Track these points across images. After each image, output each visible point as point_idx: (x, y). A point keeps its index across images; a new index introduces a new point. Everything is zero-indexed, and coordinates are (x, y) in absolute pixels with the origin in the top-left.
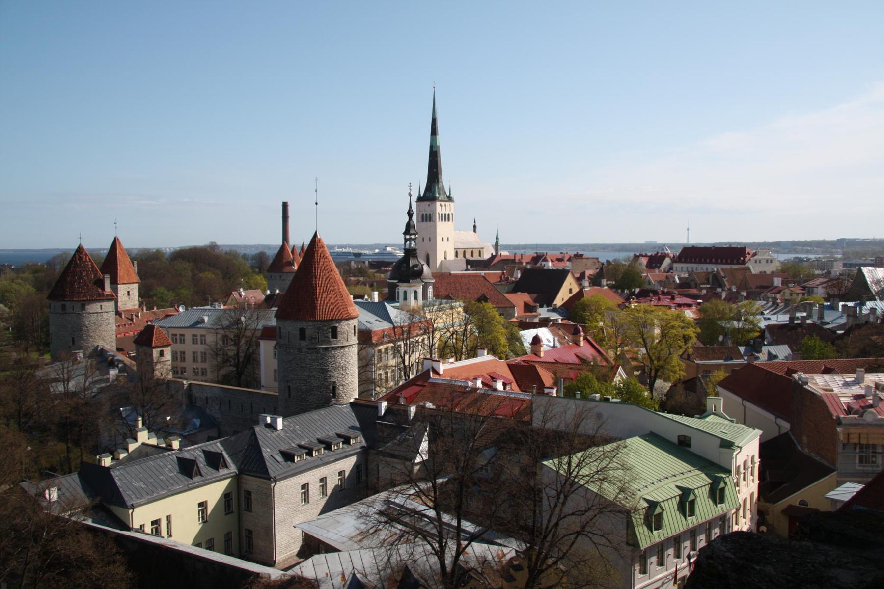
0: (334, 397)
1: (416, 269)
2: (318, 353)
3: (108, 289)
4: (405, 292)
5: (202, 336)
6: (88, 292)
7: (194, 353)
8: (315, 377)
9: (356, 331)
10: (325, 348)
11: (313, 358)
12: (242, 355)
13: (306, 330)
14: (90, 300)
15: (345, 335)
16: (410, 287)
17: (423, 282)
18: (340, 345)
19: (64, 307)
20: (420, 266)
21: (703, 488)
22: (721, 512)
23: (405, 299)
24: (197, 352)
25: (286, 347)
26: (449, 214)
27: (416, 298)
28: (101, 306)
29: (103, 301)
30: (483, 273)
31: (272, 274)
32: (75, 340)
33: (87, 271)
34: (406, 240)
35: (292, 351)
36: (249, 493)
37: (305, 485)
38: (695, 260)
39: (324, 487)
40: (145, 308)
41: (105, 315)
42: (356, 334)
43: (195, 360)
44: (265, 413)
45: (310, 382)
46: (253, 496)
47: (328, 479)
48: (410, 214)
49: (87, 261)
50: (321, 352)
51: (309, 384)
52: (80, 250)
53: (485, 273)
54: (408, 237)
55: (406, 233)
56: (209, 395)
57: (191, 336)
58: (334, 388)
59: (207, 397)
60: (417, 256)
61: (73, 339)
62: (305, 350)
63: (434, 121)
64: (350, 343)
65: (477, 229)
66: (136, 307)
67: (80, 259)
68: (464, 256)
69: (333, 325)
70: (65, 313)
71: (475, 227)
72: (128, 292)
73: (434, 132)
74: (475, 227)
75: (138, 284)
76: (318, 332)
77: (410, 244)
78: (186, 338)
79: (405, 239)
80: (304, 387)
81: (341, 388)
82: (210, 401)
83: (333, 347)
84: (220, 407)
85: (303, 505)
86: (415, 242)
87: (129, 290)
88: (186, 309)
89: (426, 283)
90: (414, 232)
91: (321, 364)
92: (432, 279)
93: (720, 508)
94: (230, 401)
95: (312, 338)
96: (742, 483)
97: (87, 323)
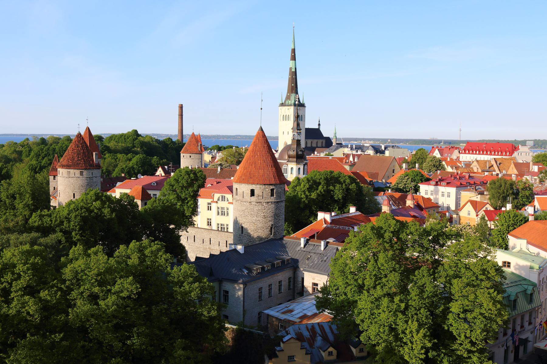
0: (271, 234)
5: (154, 195)
6: (84, 164)
8: (260, 221)
11: (260, 208)
21: (521, 293)
22: (531, 308)
27: (299, 173)
30: (330, 157)
31: (184, 154)
35: (245, 203)
36: (227, 292)
37: (260, 288)
38: (483, 152)
39: (270, 290)
41: (94, 179)
46: (230, 294)
47: (272, 285)
50: (264, 205)
52: (79, 135)
53: (333, 158)
61: (74, 194)
63: (294, 51)
64: (282, 200)
65: (321, 126)
68: (311, 145)
69: (271, 188)
71: (319, 125)
73: (294, 58)
74: (319, 125)
80: (253, 227)
83: (272, 202)
85: (259, 301)
89: (306, 163)
93: (530, 306)
94: (194, 236)
96: (541, 292)
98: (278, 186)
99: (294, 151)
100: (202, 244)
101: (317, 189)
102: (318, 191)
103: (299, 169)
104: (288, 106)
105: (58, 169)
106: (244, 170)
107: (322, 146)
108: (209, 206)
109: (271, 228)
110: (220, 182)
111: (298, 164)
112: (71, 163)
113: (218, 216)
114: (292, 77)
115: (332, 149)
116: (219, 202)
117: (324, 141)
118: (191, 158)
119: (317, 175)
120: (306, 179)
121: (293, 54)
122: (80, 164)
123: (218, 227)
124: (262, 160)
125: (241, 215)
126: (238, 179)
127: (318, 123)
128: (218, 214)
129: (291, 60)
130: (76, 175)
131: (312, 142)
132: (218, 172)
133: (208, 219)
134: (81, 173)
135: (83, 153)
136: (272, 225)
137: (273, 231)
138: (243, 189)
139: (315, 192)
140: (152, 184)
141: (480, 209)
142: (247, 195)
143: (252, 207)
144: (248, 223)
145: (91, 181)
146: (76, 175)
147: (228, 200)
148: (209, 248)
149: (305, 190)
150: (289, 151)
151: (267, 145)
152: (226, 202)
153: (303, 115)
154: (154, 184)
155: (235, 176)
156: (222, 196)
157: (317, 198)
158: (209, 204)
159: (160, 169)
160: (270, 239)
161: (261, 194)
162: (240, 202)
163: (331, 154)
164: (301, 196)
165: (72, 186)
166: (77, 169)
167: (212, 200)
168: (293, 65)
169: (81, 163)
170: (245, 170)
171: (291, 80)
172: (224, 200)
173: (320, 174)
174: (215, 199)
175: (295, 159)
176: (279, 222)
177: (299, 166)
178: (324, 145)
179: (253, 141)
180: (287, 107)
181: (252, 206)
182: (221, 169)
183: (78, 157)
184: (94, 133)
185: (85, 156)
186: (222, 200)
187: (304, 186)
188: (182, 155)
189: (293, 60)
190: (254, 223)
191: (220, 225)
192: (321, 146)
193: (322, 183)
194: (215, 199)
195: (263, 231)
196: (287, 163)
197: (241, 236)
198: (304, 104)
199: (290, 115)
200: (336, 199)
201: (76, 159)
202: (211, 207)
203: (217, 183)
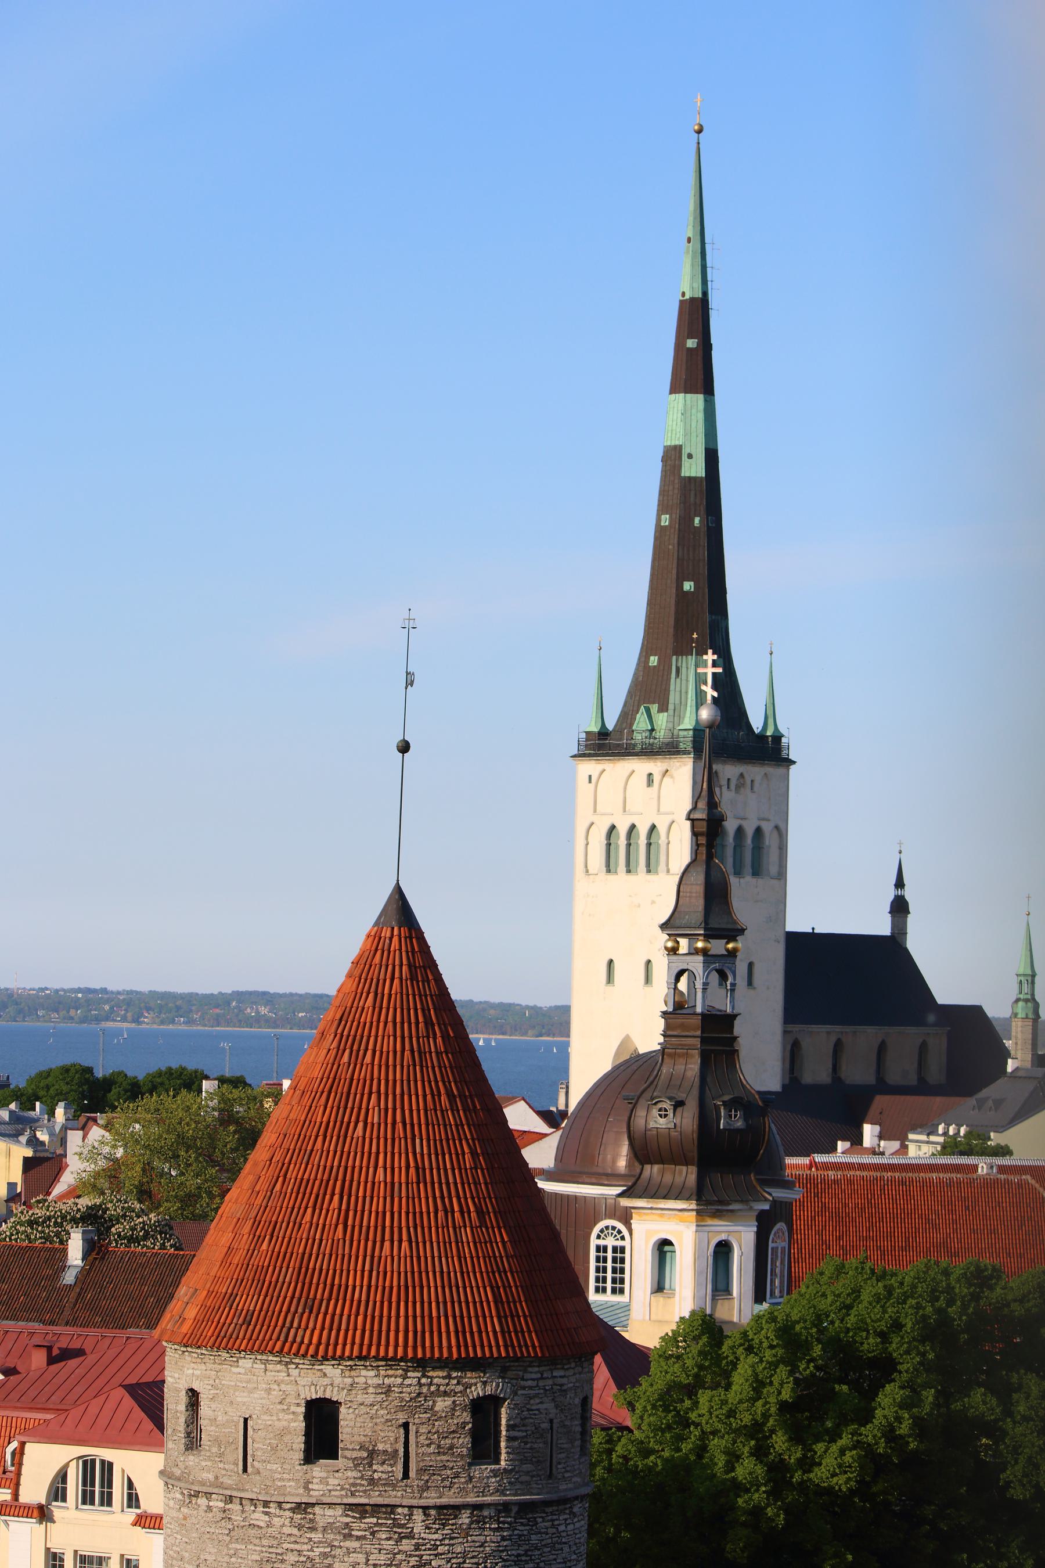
4: (663, 1247)
10: (440, 1508)
13: (343, 1410)
25: (230, 1499)
26: (758, 831)
27: (721, 1284)
35: (258, 1517)
50: (418, 1528)
53: (1002, 1169)
65: (911, 919)
68: (835, 1068)
69: (477, 1391)
71: (900, 908)
74: (900, 908)
76: (406, 1426)
89: (775, 1203)
92: (787, 1185)
95: (372, 1454)
98: (533, 1373)
99: (679, 1104)
101: (865, 1417)
102: (870, 1433)
103: (723, 1251)
104: (650, 751)
106: (259, 1240)
107: (921, 1079)
110: (80, 1353)
111: (717, 1214)
114: (683, 523)
115: (998, 1103)
116: (67, 1513)
117: (938, 1044)
119: (866, 1296)
120: (769, 1331)
121: (691, 343)
124: (399, 1162)
126: (206, 1315)
127: (890, 894)
129: (673, 390)
131: (838, 1047)
132: (69, 1278)
138: (241, 1397)
139: (845, 1440)
141: (691, 205)
142: (274, 1449)
147: (133, 1500)
149: (766, 1416)
150: (643, 1103)
151: (445, 1037)
152: (119, 1516)
153: (767, 827)
156: (88, 1465)
157: (862, 1488)
161: (389, 1439)
162: (217, 1504)
163: (995, 1139)
164: (730, 1467)
168: (687, 434)
170: (260, 1240)
171: (672, 546)
172: (107, 1500)
173: (889, 1290)
174: (34, 1491)
175: (689, 1175)
177: (721, 1229)
178: (936, 1073)
180: (641, 767)
181: (316, 1536)
182: (91, 1248)
186: (87, 1498)
187: (758, 1385)
189: (688, 389)
192: (912, 1080)
193: (907, 1365)
194: (34, 1491)
196: (625, 1202)
198: (777, 738)
199: (662, 829)
200: (1017, 1493)
203: (51, 1360)
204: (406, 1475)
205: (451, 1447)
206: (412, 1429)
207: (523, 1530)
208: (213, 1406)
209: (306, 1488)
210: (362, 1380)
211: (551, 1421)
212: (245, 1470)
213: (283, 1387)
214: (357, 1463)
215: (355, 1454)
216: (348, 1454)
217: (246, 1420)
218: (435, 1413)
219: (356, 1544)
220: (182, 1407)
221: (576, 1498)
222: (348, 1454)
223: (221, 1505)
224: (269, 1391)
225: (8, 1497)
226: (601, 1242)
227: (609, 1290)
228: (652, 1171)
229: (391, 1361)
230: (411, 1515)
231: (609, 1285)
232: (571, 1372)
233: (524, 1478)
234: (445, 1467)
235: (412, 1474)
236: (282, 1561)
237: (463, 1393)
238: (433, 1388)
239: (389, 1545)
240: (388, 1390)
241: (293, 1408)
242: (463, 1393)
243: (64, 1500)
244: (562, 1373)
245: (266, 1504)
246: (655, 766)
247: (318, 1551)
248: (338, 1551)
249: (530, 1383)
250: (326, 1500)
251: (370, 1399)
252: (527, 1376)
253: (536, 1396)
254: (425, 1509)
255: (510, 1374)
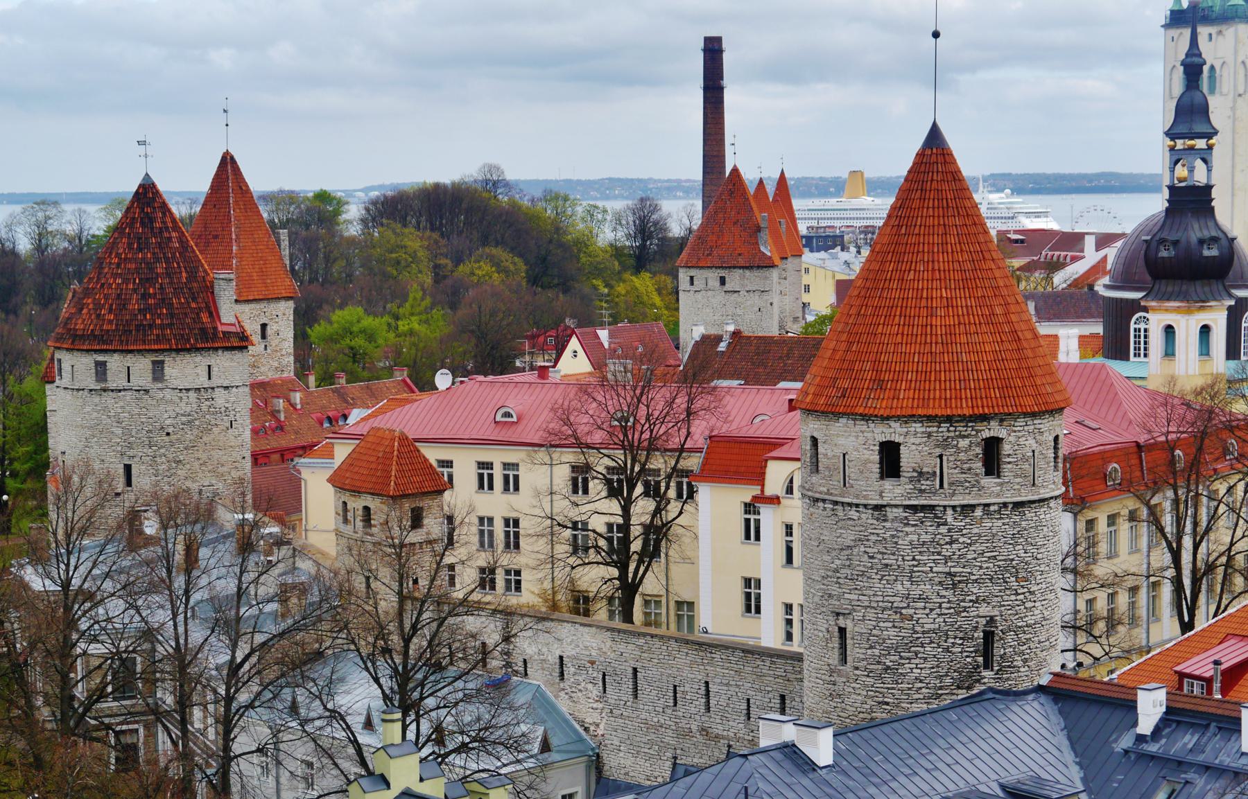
1: (1206, 253)
2: (939, 526)
3: (229, 312)
4: (1169, 330)
5: (506, 466)
6: (170, 325)
7: (481, 519)
8: (926, 600)
9: (1060, 454)
10: (963, 507)
11: (925, 538)
12: (636, 530)
13: (902, 447)
14: (178, 351)
15: (1026, 466)
16: (1189, 311)
17: (1231, 296)
18: (1010, 498)
19: (101, 370)
20: (1224, 242)
23: (1169, 352)
24: (491, 520)
28: (209, 366)
29: (216, 349)
31: (693, 272)
32: (134, 471)
33: (167, 261)
34: (1176, 158)
35: (853, 513)
40: (312, 379)
41: (221, 398)
42: (1061, 465)
43: (486, 539)
44: (783, 712)
45: (911, 618)
48: (1193, 69)
49: (167, 228)
50: (950, 519)
51: (908, 624)
52: (147, 195)
54: (1180, 144)
55: (1171, 134)
56: (569, 652)
57: (475, 466)
58: (989, 637)
59: (561, 658)
60: (1213, 208)
61: (128, 468)
62: (899, 512)
66: (285, 375)
67: (148, 221)
69: (986, 434)
70: (105, 390)
72: (264, 326)
75: (291, 304)
76: (941, 457)
77: (1191, 170)
78: (455, 470)
79: (1172, 149)
80: (892, 632)
81: (1010, 637)
82: (570, 670)
83: (988, 505)
84: (605, 692)
86: (1205, 161)
87: (265, 320)
88: (453, 383)
89: (1240, 301)
90: (1200, 128)
91: (947, 559)
95: (921, 474)
97: (168, 422)
100: (669, 711)
103: (1205, 330)
105: (57, 356)
108: (752, 517)
109: (989, 637)
112: (110, 322)
113: (789, 571)
118: (728, 287)
122: (150, 326)
123: (789, 622)
125: (836, 571)
128: (789, 560)
130: (136, 381)
133: (747, 582)
134: (158, 371)
135: (168, 275)
136: (991, 620)
137: (998, 651)
138: (841, 441)
140: (499, 418)
142: (862, 472)
143: (886, 530)
144: (871, 614)
145: (204, 408)
146: (136, 381)
148: (704, 731)
154: (508, 415)
155: (808, 376)
158: (750, 508)
159: (574, 344)
160: (981, 693)
165: (119, 431)
166: (139, 351)
167: (756, 490)
169: (158, 322)
170: (850, 343)
176: (1029, 605)
179: (892, 200)
181: (888, 525)
183: (145, 296)
184: (259, 179)
185: (177, 293)
188: (683, 275)
190: (897, 611)
191: (796, 610)
195: (947, 650)
197: (840, 674)
201: (134, 305)
202: (758, 522)
204: (941, 486)
205: (970, 469)
206: (945, 458)
207: (1017, 518)
208: (826, 446)
209: (881, 496)
210: (913, 429)
211: (1033, 451)
212: (845, 485)
213: (865, 434)
214: (911, 480)
215: (909, 475)
216: (905, 474)
217: (844, 455)
218: (958, 449)
219: (913, 529)
220: (808, 447)
221: (1052, 498)
222: (905, 474)
223: (831, 506)
224: (857, 437)
225: (759, 492)
226: (1137, 326)
227: (1142, 355)
228: (1163, 286)
229: (930, 418)
230: (945, 510)
231: (1142, 352)
232: (1046, 421)
233: (1017, 487)
234: (966, 481)
235: (946, 485)
236: (868, 540)
237: (976, 436)
238: (957, 433)
239: (930, 529)
240: (929, 435)
241: (872, 447)
242: (976, 436)
243: (792, 493)
244: (1039, 421)
245: (857, 505)
246: (1213, 30)
247: (888, 534)
248: (900, 534)
249: (1019, 428)
250: (893, 502)
251: (918, 441)
252: (1016, 424)
253: (1023, 436)
254: (954, 507)
255: (1005, 423)
